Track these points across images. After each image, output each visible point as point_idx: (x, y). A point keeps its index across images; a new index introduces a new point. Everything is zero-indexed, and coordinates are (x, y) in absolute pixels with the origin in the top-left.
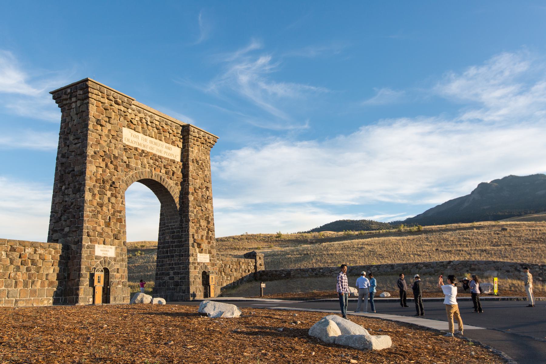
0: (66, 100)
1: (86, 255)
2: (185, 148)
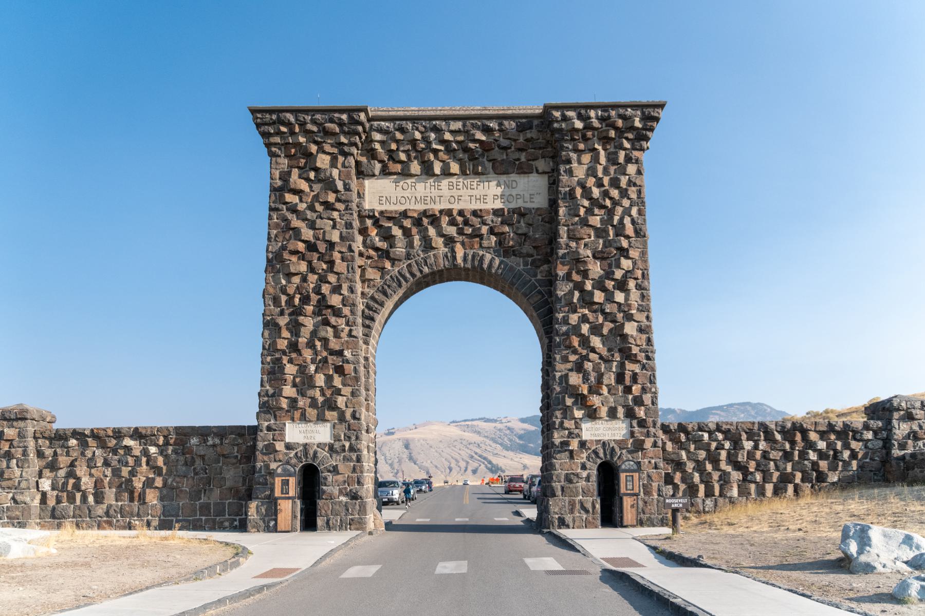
1: (266, 443)
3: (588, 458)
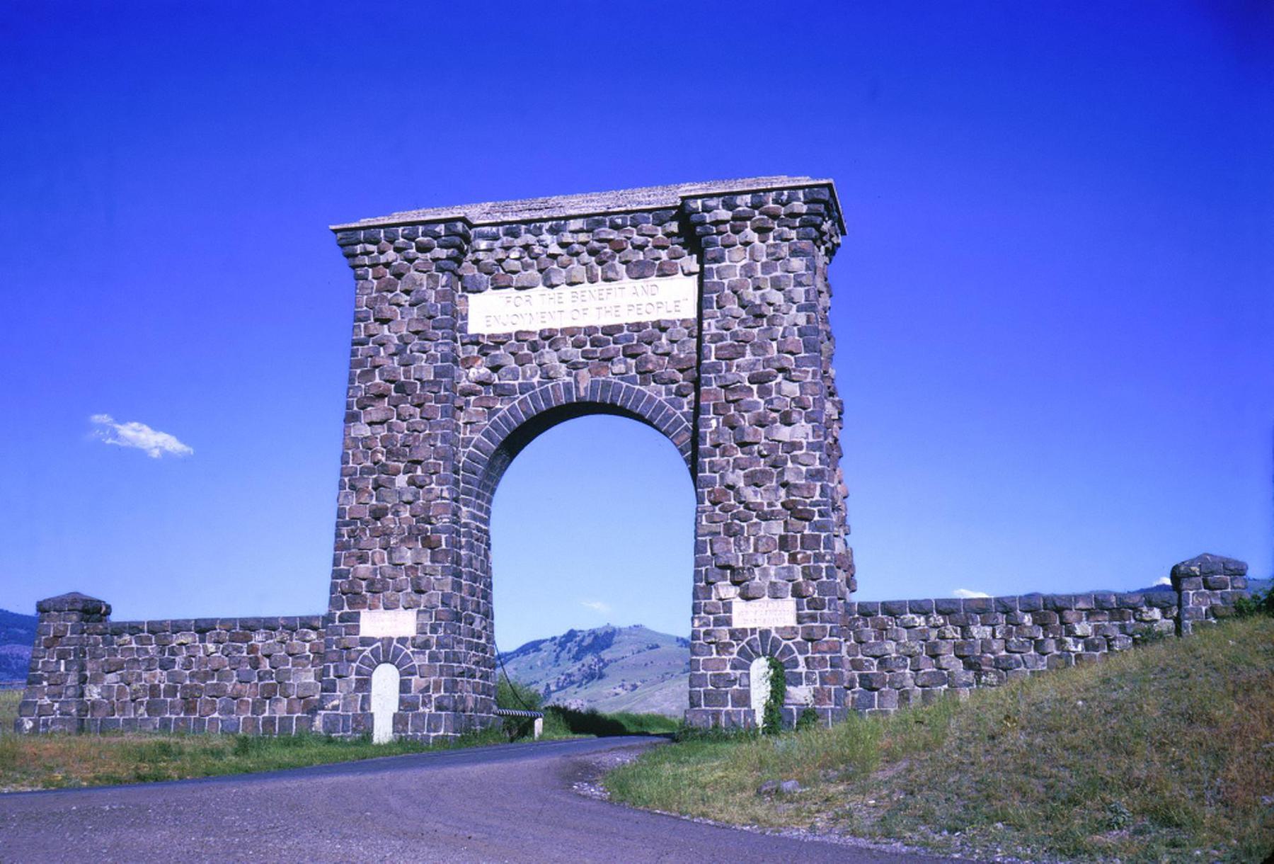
3: (739, 654)
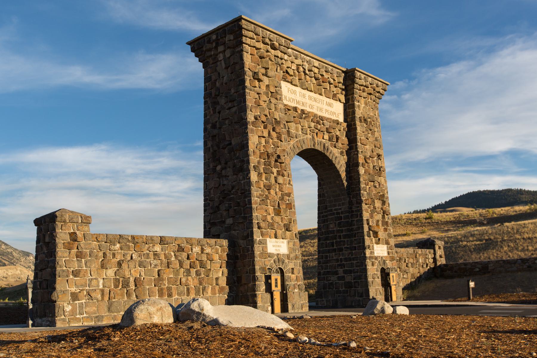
0: (210, 50)
1: (259, 252)
2: (349, 103)
